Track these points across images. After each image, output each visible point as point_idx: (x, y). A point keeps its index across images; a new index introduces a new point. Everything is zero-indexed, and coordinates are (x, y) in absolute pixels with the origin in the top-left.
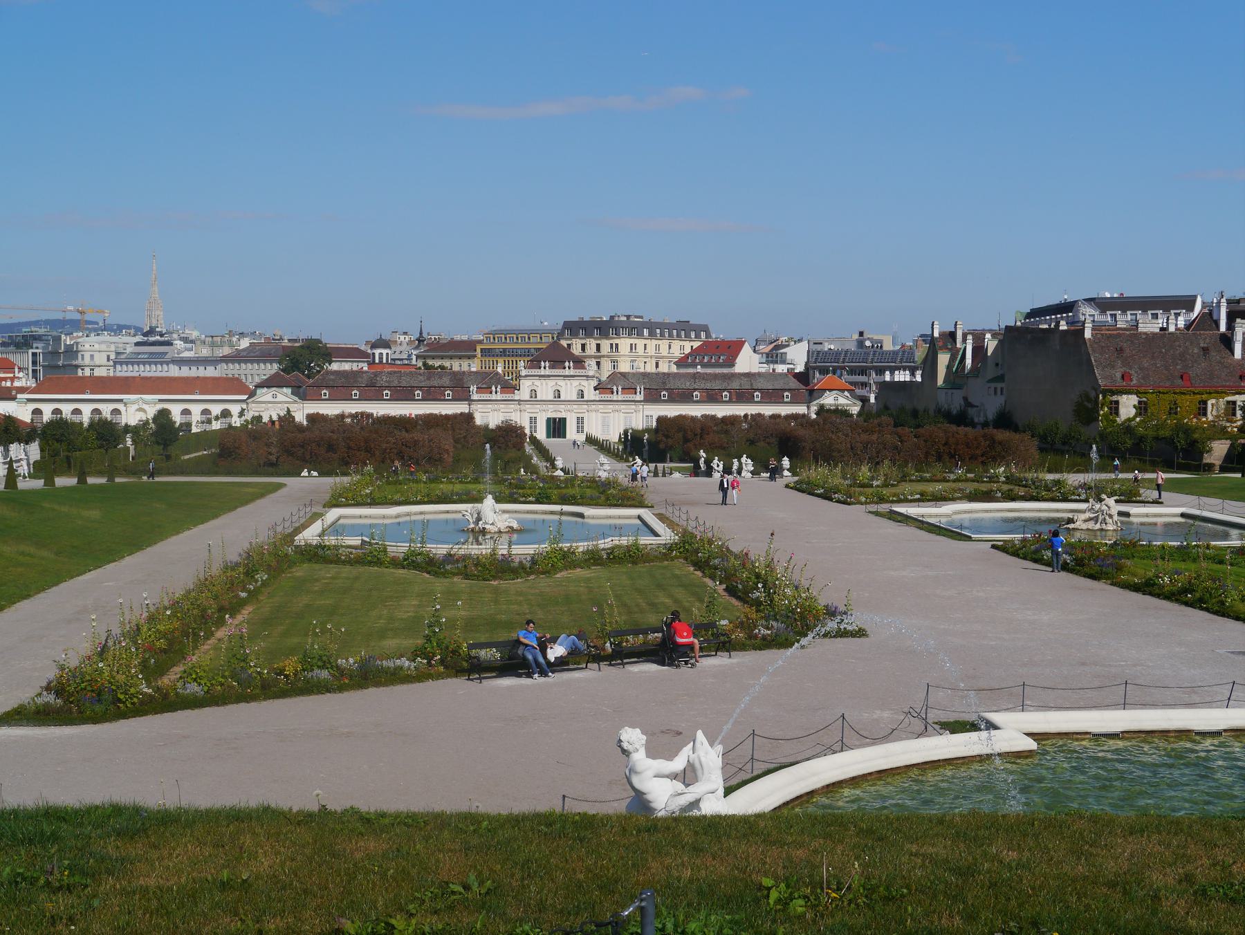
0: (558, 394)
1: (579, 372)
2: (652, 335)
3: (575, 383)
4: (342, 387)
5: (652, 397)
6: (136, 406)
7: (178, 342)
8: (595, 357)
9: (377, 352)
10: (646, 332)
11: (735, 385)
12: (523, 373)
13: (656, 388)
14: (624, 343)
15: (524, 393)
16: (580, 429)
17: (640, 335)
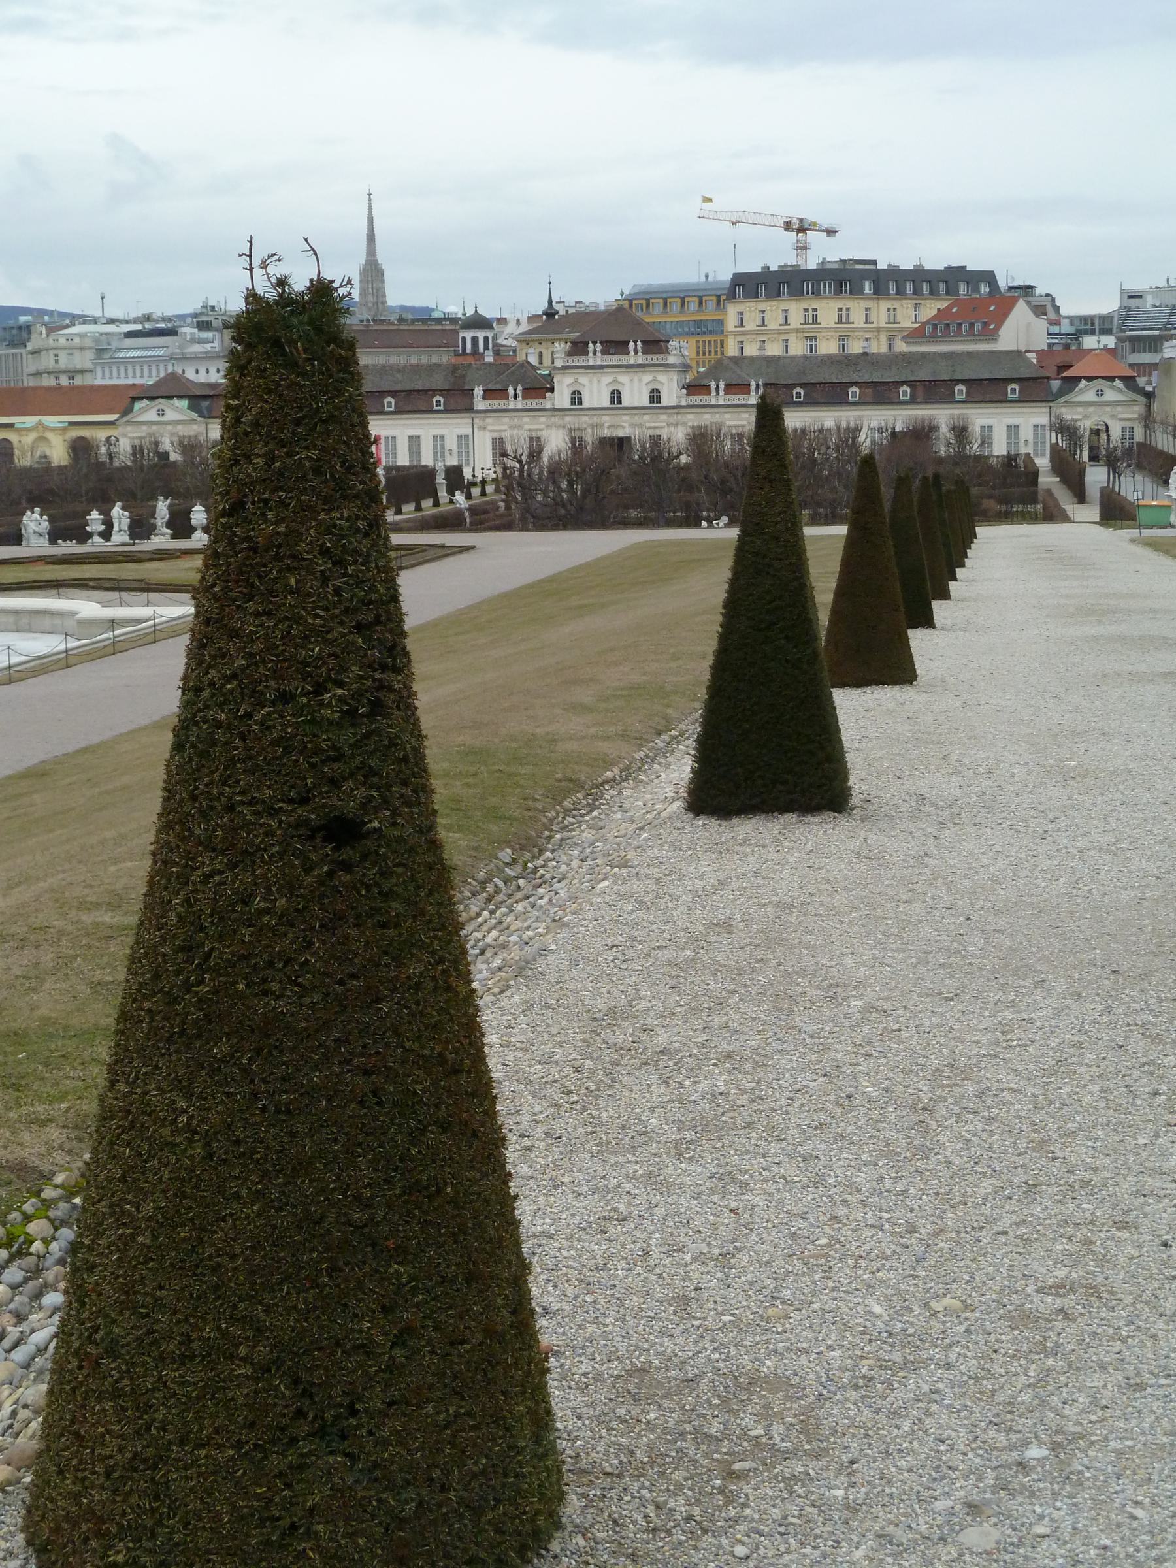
0: (616, 397)
3: (647, 378)
8: (779, 332)
10: (868, 287)
11: (923, 375)
15: (561, 397)
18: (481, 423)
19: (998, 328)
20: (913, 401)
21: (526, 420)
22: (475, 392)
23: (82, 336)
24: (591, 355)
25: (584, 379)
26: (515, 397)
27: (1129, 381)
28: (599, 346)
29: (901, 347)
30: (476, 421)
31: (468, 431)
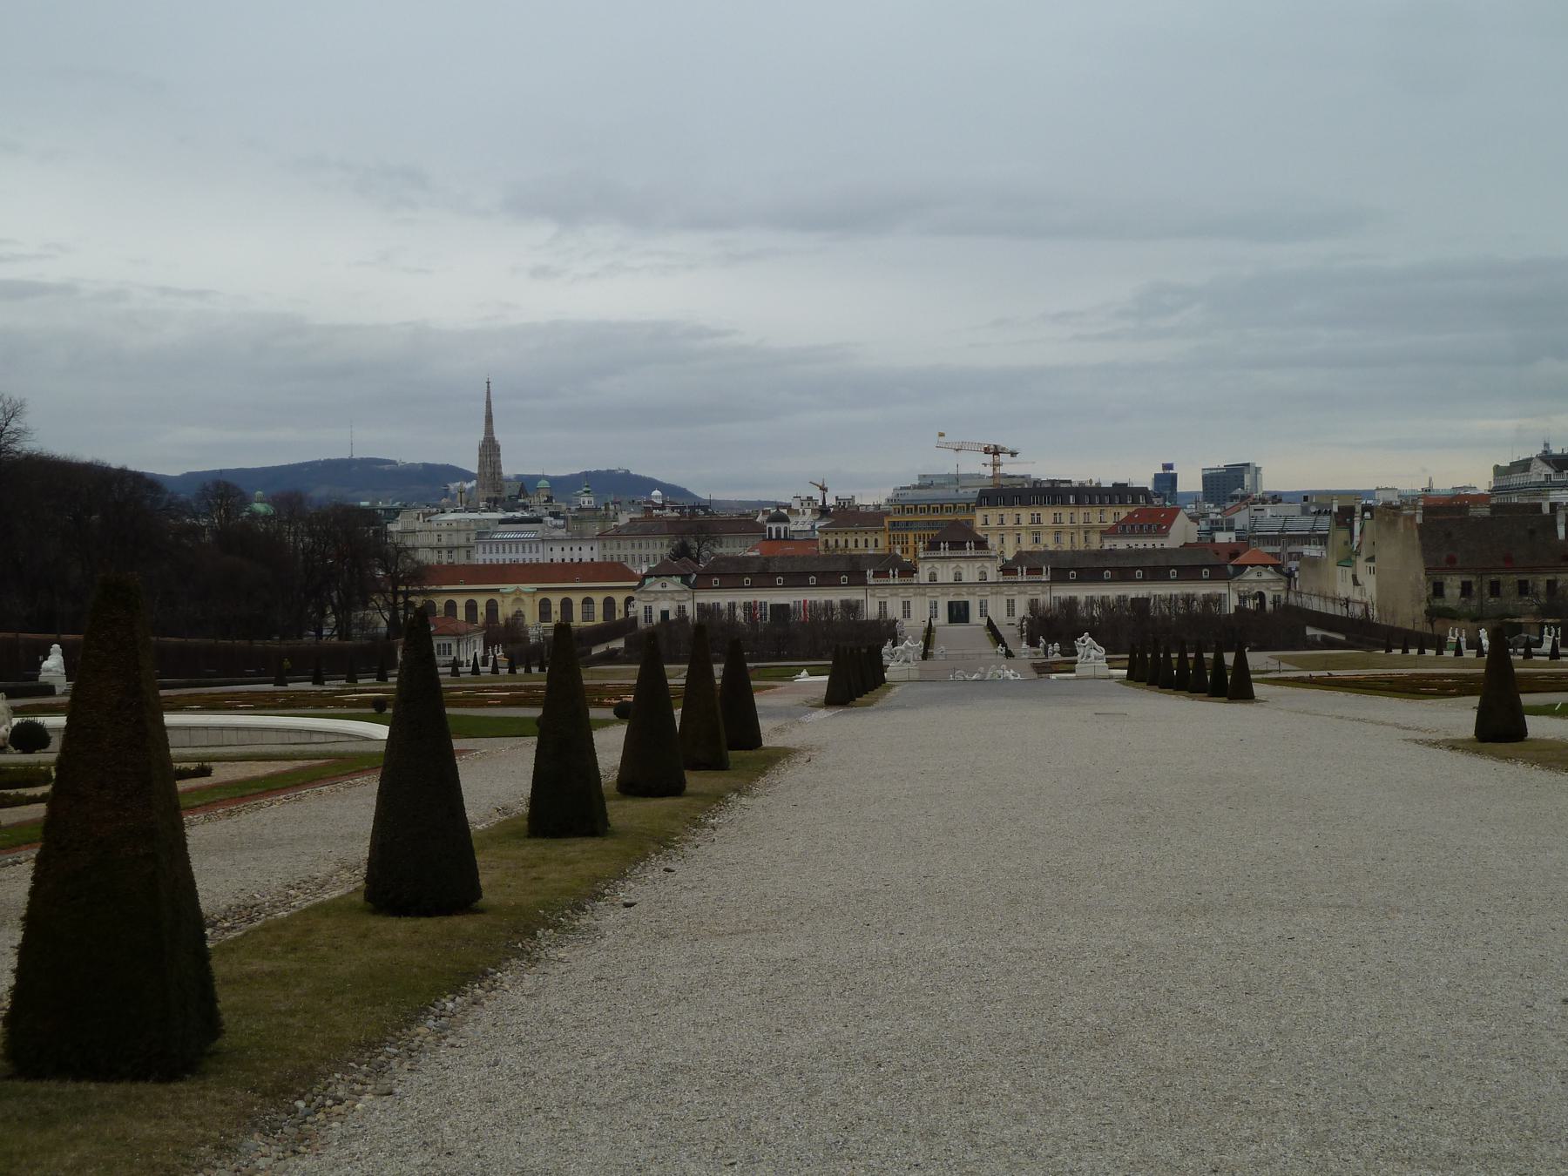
0: (958, 577)
1: (981, 553)
2: (1078, 502)
3: (978, 565)
4: (732, 574)
5: (1060, 575)
6: (512, 597)
7: (549, 519)
9: (774, 526)
12: (921, 555)
13: (1064, 568)
14: (1047, 515)
15: (923, 576)
16: (983, 613)
17: (1065, 503)
19: (1168, 528)
20: (1144, 579)
23: (458, 521)
25: (937, 565)
27: (1278, 568)
29: (1095, 543)
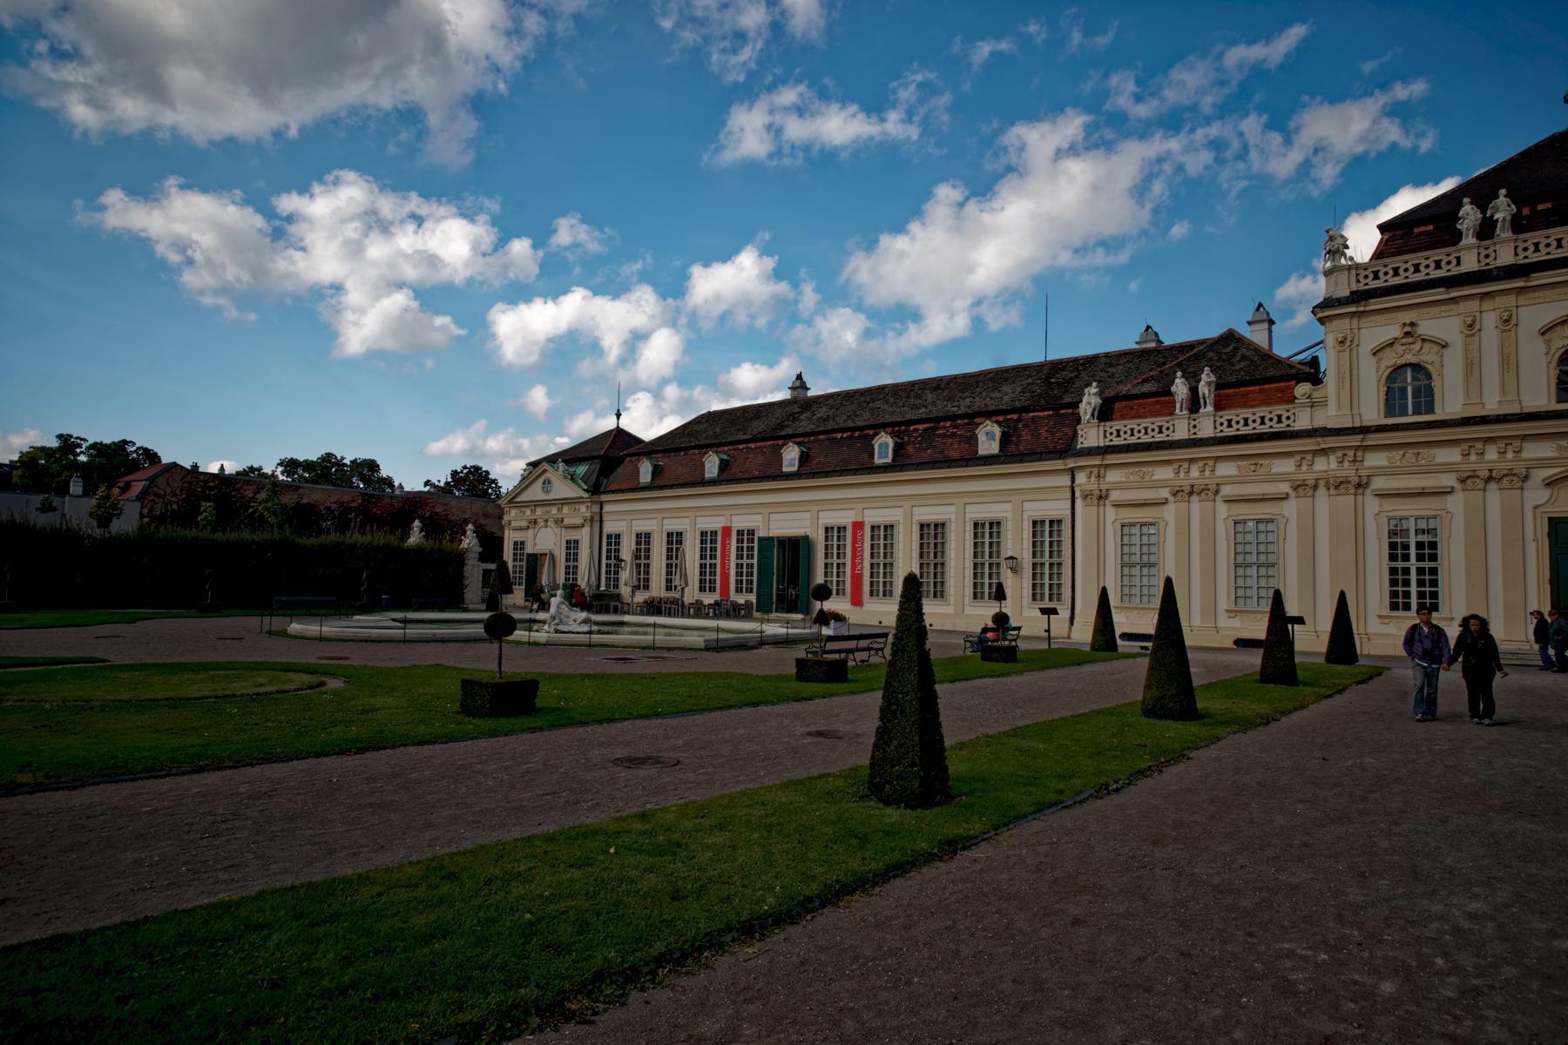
18: (1093, 486)
21: (1226, 470)
22: (1082, 406)
24: (1469, 240)
26: (1194, 405)
28: (1502, 208)
30: (1081, 478)
31: (1060, 509)
